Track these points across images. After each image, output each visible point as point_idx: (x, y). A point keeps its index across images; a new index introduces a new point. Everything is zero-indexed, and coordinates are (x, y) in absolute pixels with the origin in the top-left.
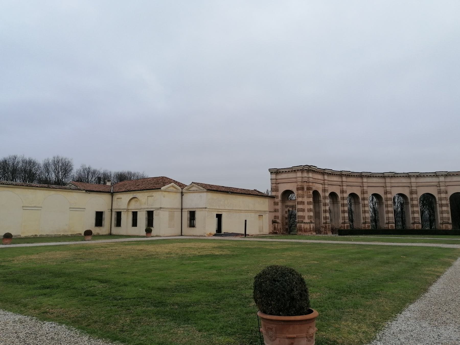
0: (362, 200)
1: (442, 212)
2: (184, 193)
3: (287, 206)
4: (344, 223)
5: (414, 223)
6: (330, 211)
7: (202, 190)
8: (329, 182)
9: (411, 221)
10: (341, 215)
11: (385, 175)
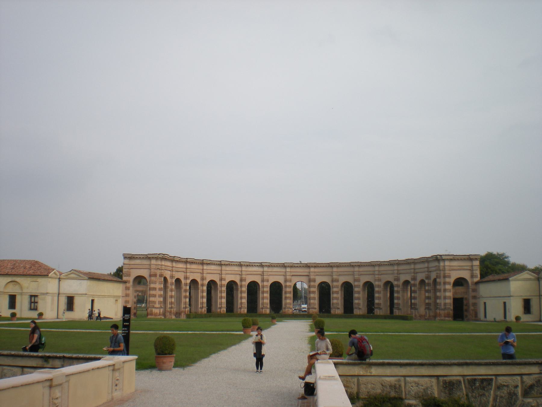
3: (136, 291)
4: (186, 308)
7: (83, 278)
8: (176, 269)
11: (222, 263)
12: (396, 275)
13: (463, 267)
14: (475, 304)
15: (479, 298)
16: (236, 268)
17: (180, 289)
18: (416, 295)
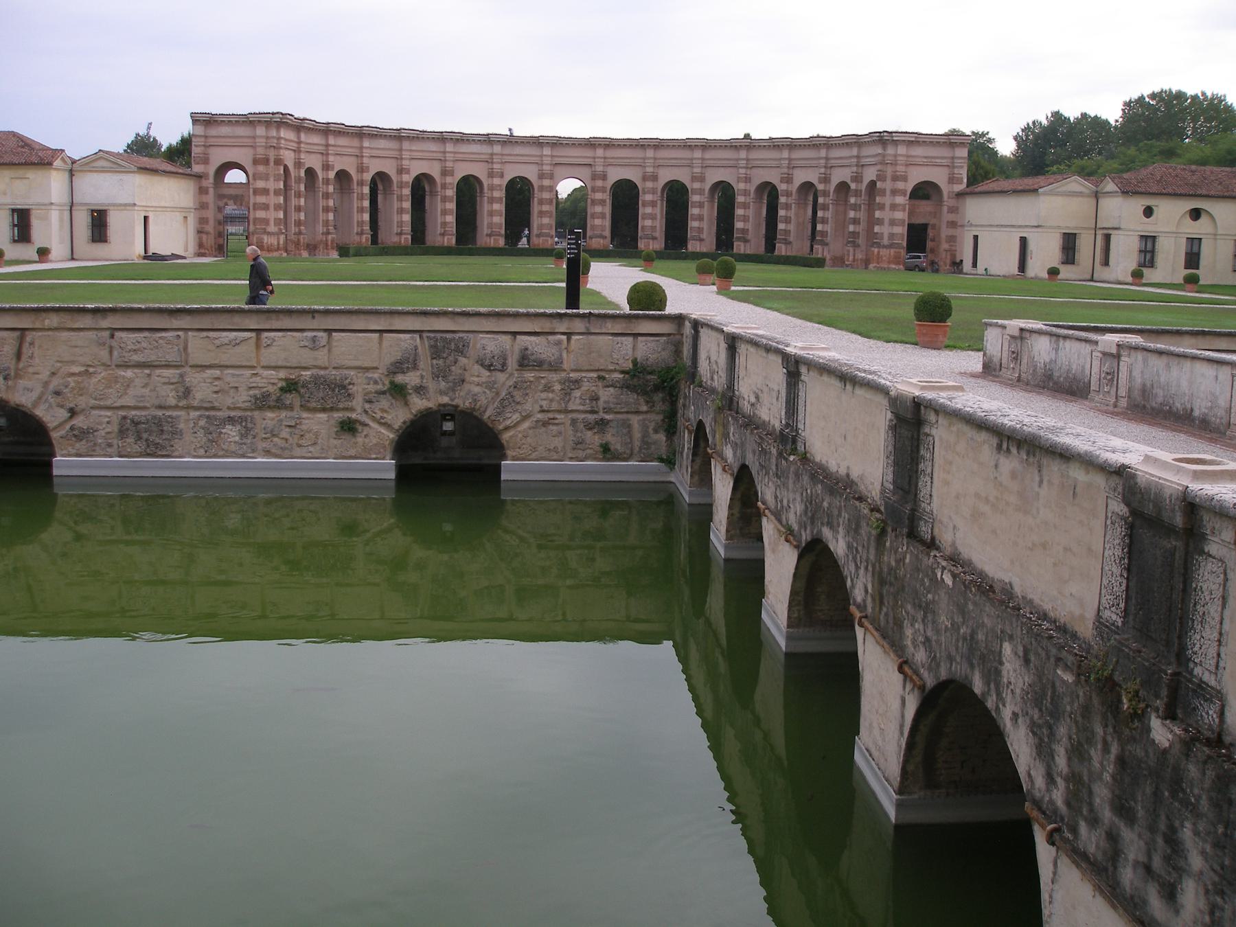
0: (358, 185)
1: (491, 214)
2: (76, 171)
5: (443, 235)
6: (335, 210)
9: (439, 230)
10: (322, 216)
12: (786, 170)
13: (933, 160)
14: (952, 239)
15: (962, 226)
16: (433, 147)
17: (315, 191)
18: (829, 214)
